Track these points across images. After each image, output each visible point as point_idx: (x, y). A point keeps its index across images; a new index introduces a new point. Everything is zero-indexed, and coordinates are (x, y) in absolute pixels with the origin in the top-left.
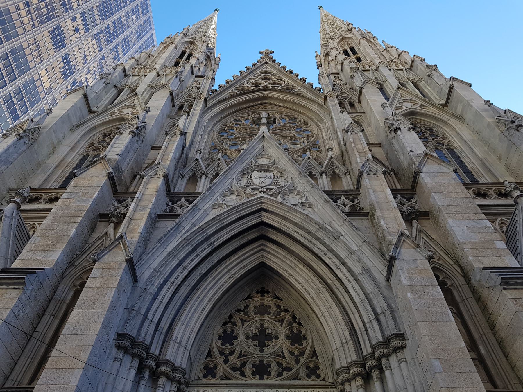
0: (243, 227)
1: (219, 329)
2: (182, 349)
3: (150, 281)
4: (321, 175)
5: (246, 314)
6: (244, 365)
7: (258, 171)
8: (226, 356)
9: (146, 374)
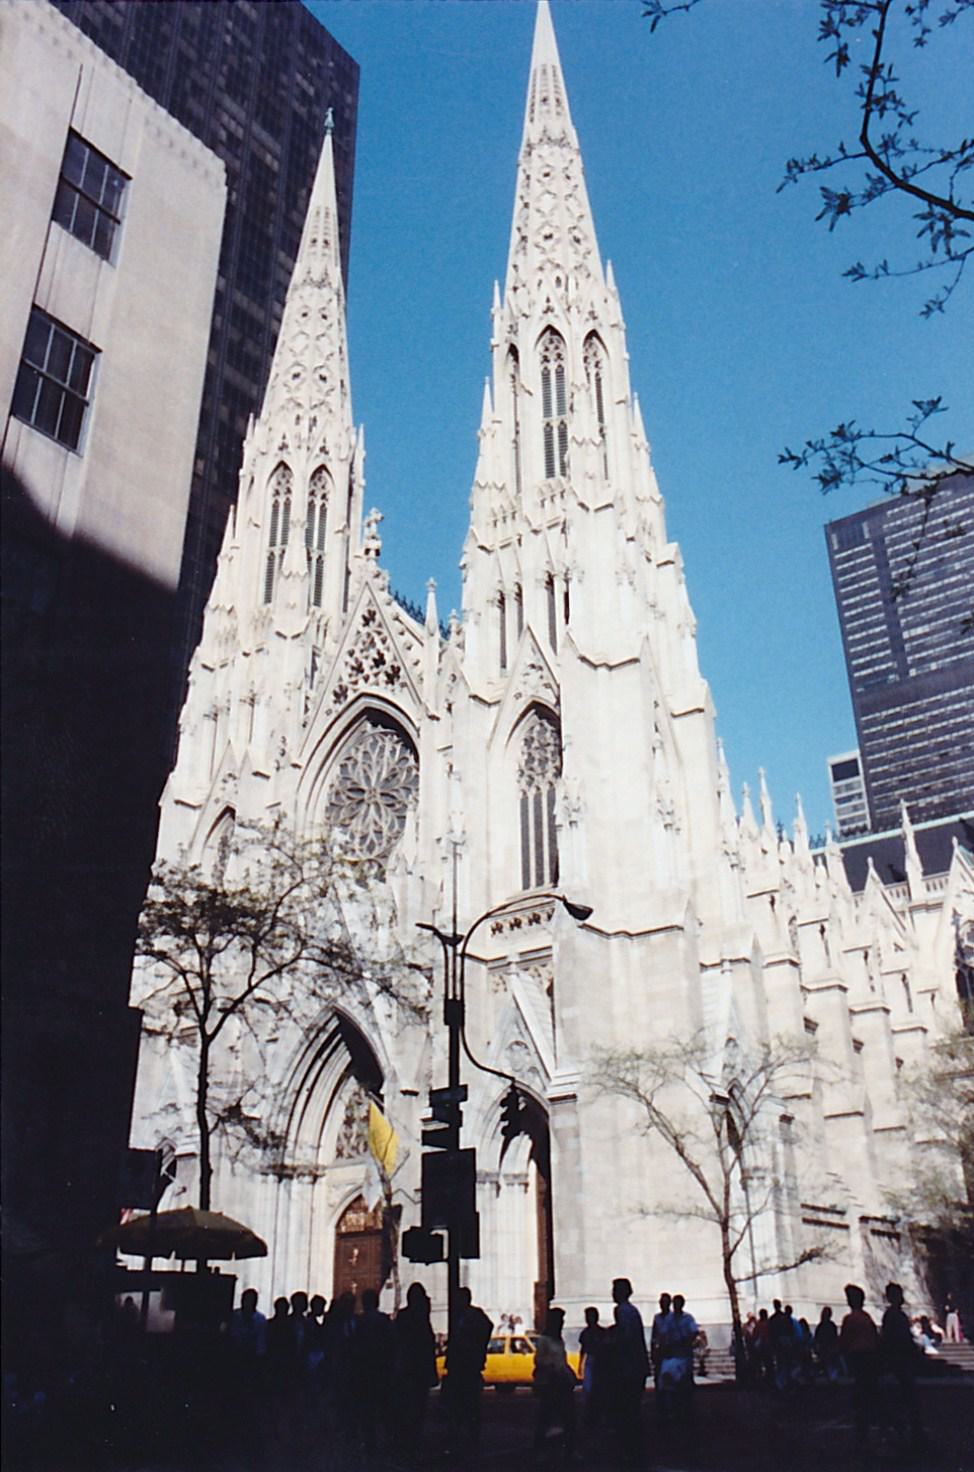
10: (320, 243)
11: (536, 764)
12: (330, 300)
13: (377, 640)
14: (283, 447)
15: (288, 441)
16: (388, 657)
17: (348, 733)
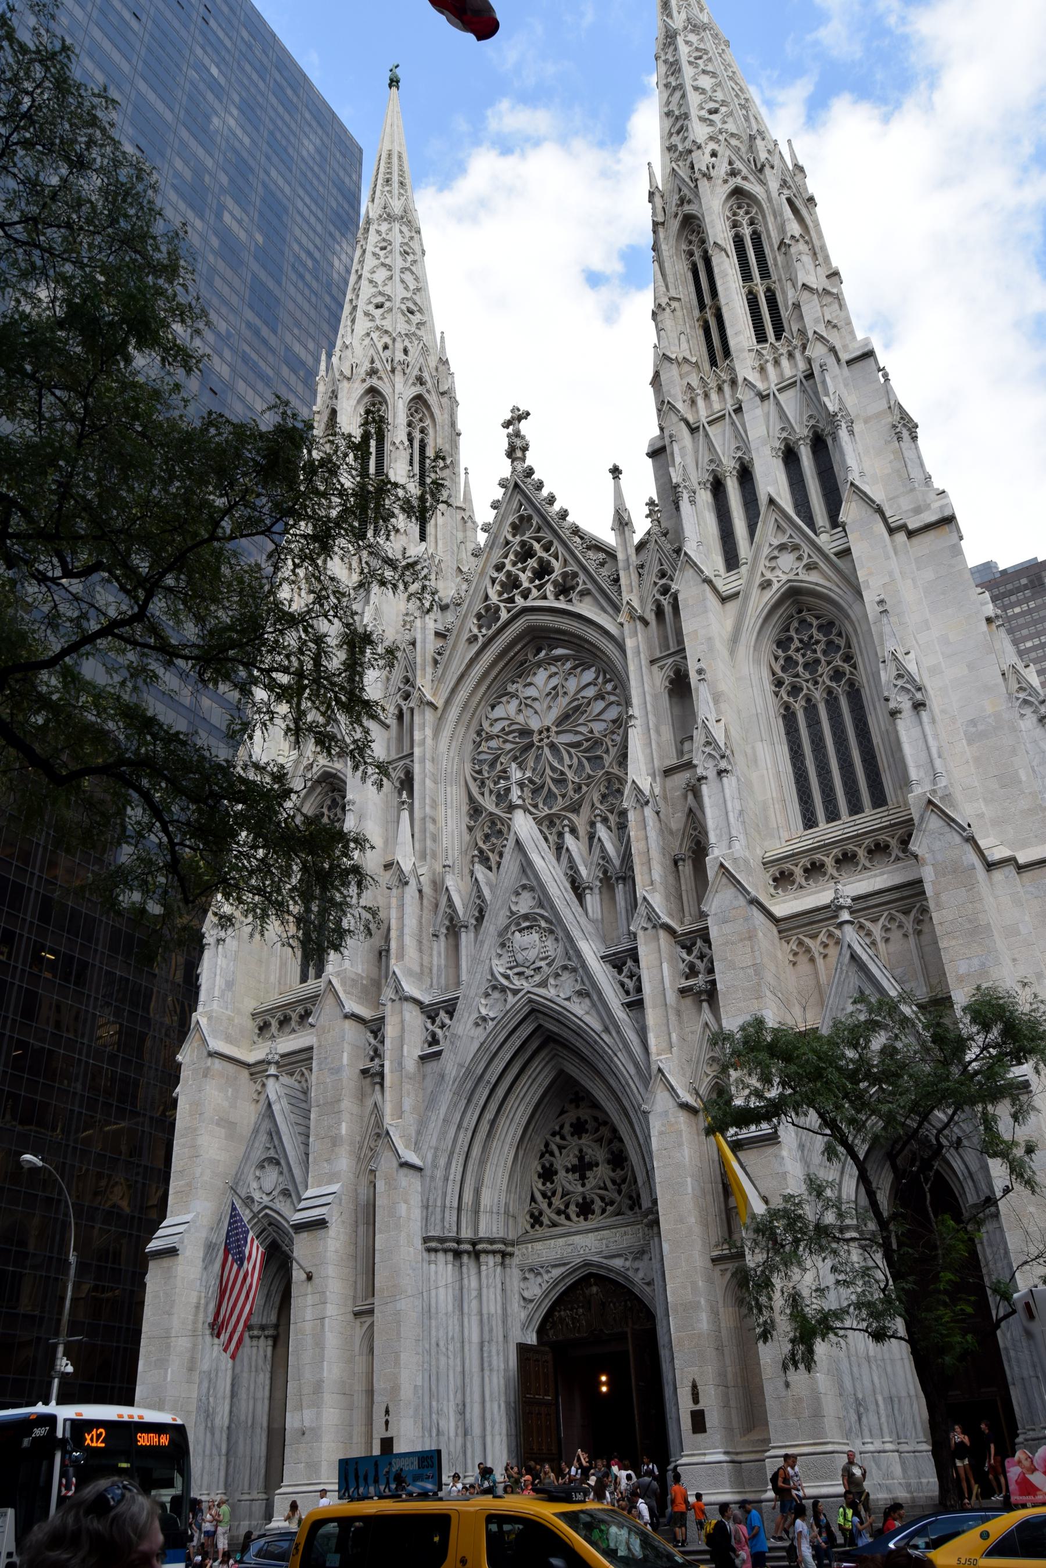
0: (518, 1043)
1: (536, 1166)
2: (495, 1216)
3: (435, 1166)
4: (617, 879)
5: (563, 1138)
6: (567, 1206)
7: (520, 931)
8: (549, 1198)
9: (465, 1259)
10: (396, 185)
11: (800, 669)
12: (412, 238)
13: (537, 546)
14: (373, 372)
15: (378, 365)
16: (556, 565)
17: (501, 664)
